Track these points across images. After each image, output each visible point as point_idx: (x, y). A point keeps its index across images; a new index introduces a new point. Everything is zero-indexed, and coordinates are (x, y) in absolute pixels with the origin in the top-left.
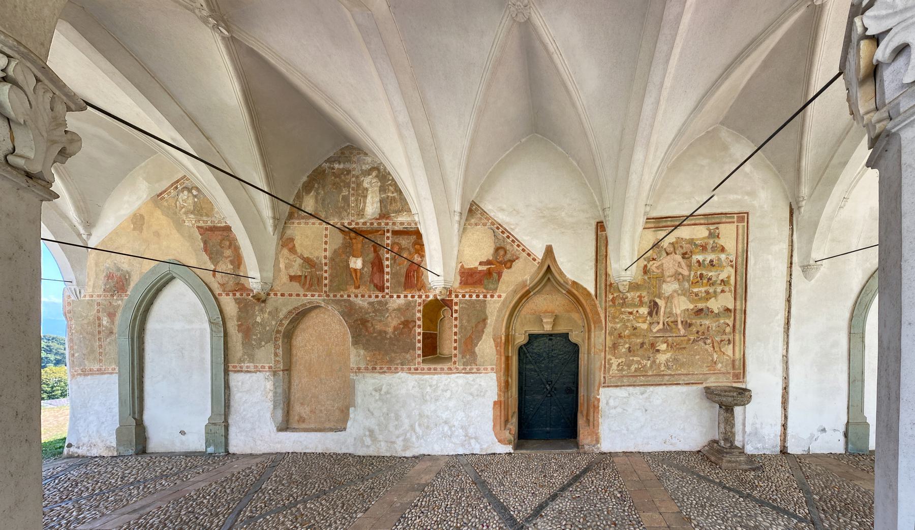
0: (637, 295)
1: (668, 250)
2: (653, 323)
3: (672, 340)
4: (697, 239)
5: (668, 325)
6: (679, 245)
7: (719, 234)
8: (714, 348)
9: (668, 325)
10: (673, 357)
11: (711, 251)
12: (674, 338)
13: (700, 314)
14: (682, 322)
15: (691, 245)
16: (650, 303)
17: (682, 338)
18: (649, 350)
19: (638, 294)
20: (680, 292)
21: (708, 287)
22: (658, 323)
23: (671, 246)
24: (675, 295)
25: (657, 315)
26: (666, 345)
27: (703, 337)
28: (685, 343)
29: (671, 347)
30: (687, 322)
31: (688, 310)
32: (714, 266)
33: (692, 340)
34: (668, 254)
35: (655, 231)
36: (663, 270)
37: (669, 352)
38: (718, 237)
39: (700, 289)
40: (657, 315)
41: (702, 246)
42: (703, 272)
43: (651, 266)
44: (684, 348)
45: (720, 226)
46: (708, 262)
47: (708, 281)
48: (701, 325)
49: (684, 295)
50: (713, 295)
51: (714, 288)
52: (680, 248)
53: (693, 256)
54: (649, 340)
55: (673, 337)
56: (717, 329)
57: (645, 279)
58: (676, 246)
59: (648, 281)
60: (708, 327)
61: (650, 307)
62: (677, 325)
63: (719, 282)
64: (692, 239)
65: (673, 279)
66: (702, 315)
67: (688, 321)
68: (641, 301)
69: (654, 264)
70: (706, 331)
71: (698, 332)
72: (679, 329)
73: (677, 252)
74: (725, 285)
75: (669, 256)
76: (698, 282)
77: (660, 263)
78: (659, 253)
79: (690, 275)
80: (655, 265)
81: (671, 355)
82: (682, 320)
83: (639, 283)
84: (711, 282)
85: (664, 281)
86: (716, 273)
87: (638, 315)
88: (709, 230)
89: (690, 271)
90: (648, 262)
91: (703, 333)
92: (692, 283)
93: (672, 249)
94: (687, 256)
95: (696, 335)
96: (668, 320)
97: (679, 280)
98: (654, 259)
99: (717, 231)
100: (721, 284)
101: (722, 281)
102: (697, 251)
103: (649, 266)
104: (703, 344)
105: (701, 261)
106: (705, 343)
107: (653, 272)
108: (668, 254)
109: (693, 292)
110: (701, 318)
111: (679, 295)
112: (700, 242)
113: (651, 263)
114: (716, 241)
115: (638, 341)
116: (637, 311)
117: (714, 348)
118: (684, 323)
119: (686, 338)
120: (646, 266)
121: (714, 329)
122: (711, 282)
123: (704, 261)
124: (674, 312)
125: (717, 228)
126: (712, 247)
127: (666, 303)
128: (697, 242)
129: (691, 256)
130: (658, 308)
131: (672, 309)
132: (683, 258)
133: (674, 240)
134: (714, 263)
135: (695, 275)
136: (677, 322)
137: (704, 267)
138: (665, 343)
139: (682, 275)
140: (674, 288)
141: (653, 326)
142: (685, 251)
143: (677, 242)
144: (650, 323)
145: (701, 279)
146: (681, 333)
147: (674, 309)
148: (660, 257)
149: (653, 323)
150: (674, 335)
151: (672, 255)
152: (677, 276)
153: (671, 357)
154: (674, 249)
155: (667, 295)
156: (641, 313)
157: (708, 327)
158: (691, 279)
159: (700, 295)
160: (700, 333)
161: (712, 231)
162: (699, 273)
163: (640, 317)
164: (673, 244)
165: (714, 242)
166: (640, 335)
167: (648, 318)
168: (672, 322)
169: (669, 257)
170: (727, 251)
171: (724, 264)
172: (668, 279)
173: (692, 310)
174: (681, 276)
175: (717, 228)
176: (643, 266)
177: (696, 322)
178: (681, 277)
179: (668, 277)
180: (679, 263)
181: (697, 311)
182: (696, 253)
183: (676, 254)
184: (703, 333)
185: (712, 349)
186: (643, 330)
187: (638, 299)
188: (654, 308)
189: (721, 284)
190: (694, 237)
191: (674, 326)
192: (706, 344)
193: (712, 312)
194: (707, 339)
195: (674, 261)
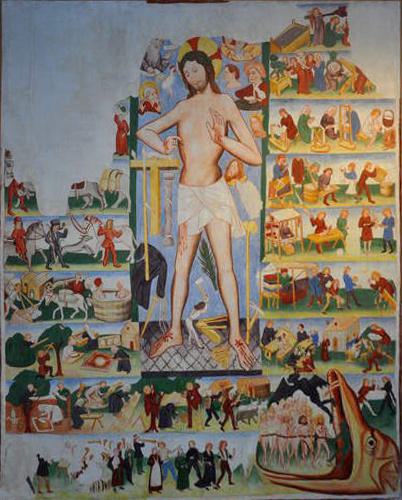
7: (347, 30)
32: (335, 136)
68: (108, 245)
76: (288, 188)
84: (328, 189)
94: (251, 99)
99: (342, 20)
123: (305, 119)
132: (243, 105)
134: (336, 128)
136: (227, 323)
145: (298, 180)
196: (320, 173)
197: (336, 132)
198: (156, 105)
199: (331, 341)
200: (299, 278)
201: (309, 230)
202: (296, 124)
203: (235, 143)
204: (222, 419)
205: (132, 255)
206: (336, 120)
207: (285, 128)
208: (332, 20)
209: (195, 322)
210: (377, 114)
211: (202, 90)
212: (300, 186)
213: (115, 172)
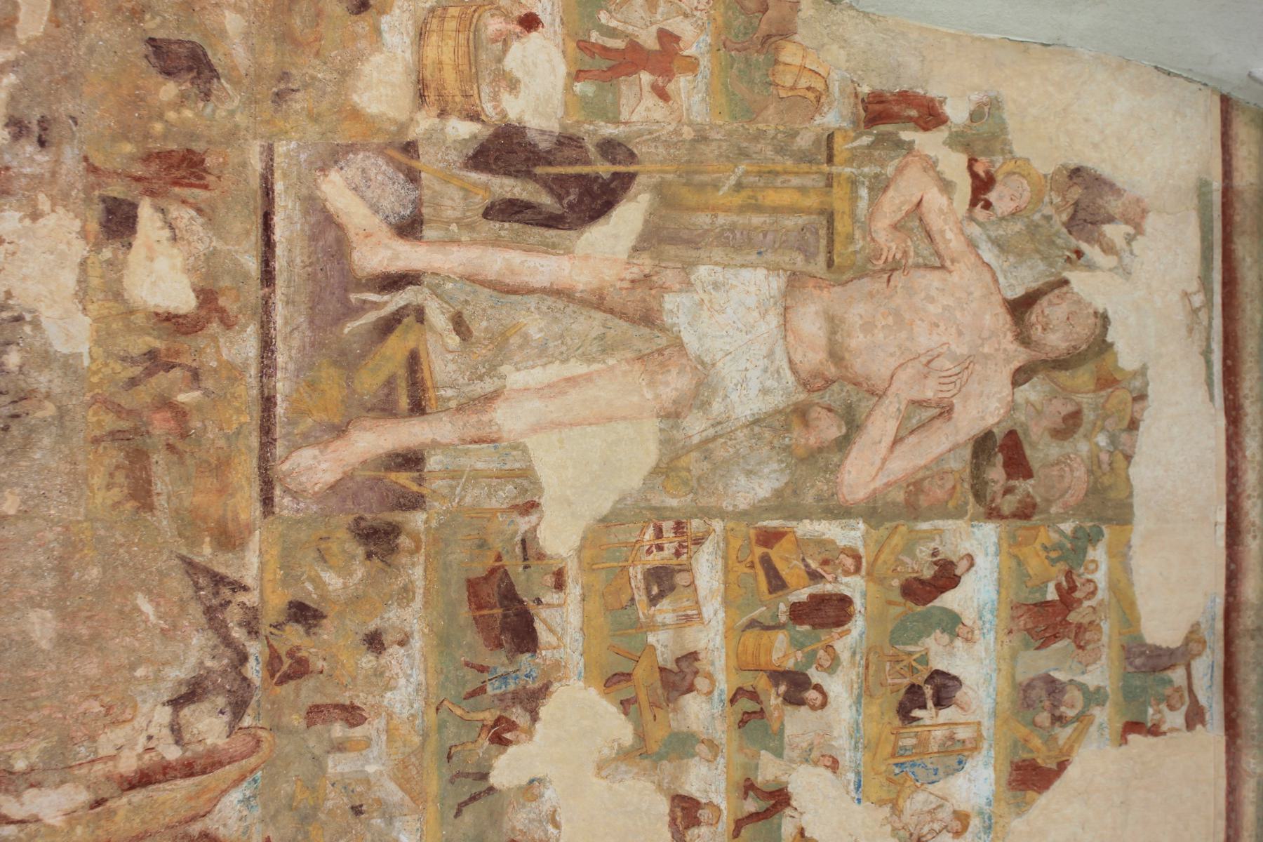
0: (682, 27)
1: (1052, 311)
2: (413, 177)
3: (234, 372)
4: (1121, 554)
5: (388, 326)
6: (1086, 400)
7: (1155, 731)
8: (143, 779)
9: (388, 326)
10: (42, 380)
11: (1022, 678)
12: (249, 389)
13: (481, 624)
14: (411, 460)
15: (1081, 509)
16: (609, 148)
17: (245, 469)
18: (124, 135)
19: (695, 42)
20: (695, 426)
21: (724, 685)
22: (409, 228)
23: (1083, 330)
24: (675, 384)
25: (488, 213)
26: (182, 300)
27: (254, 670)
28: (200, 497)
29: (155, 362)
30: (415, 502)
31: (530, 507)
32: (904, 712)
33: (223, 565)
34: (1020, 308)
35: (1202, 188)
36: (893, 268)
37: (102, 337)
38: (1134, 727)
39: (713, 609)
40: (488, 213)
41: (1068, 598)
42: (857, 626)
43: (930, 165)
44: (142, 494)
45: (1212, 735)
46: (939, 663)
47: (777, 676)
48: (375, 642)
49: (665, 471)
50: (658, 733)
51: (721, 731)
52: (1062, 408)
53: (989, 532)
54: (232, 135)
55: (267, 368)
56: (335, 800)
57: (818, 100)
58: (1083, 377)
59: (804, 141)
60: (352, 715)
61: (568, 141)
62: (385, 409)
63: (769, 770)
64: (1122, 514)
65: (813, 358)
66: (472, 644)
67: (417, 520)
69: (946, 186)
70: (308, 692)
71: (303, 613)
72: (339, 431)
73: (1031, 392)
74: (739, 825)
75: (1005, 319)
76: (777, 583)
77: (952, 240)
78: (1033, 229)
79: (839, 512)
80: (935, 199)
81: (68, 365)
82: (433, 462)
83: (790, 54)
84: (773, 700)
85: (795, 281)
86: (842, 743)
87: (494, 25)
88: (1183, 655)
89: (873, 512)
90: (961, 141)
91: (300, 669)
92: (769, 538)
93: (1056, 341)
94: (996, 473)
95: (277, 601)
96: (438, 317)
97: (801, 413)
98: (982, 185)
99: (1176, 719)
100: (749, 787)
101: (779, 799)
102: (1035, 564)
103: (928, 142)
104: (178, 674)
105: (949, 600)
106: (190, 694)
107: (880, 186)
108: (1020, 308)
109: (689, 542)
110: (444, 641)
111: (672, 416)
112: (1100, 577)
113: (954, 165)
114: (1101, 715)
115: (233, 22)
116: (530, 22)
117: (143, 779)
118: (404, 479)
119: (246, 504)
120: (931, 116)
121: (338, 765)
122: (773, 700)
123: (952, 623)
124: (515, 378)
125: (1195, 717)
126: (1053, 688)
127: (597, 302)
128: (1098, 553)
129: (993, 514)
130: (552, 221)
131: (543, 353)
132: (983, 445)
133: (1126, 357)
134: (926, 715)
135: (830, 556)
136: (418, 408)
137: (903, 632)
138: (207, 296)
139: (844, 443)
140: (728, 371)
141: (379, 169)
142: (1034, 456)
143: (1107, 381)
144: (410, 148)
145: (798, 613)
146: (306, 456)
147: (538, 375)
148: (1001, 245)
149: (413, 177)
150: (282, 386)
151: (1008, 342)
152: (835, 396)
153: (46, 358)
154: (1060, 364)
155: (675, 308)
156: (512, 62)
157: (352, 715)
158: (806, 528)
159: (665, 611)
160: (294, 635)
161: (1178, 675)
162: (852, 586)
163: (474, 45)
164: (1100, 346)
165: (1094, 697)
166: (286, 38)
167: (462, 129)
168: (414, 361)
169: (998, 319)
170: (1021, 807)
171: (917, 803)
172: (809, 322)
173: (528, 548)
174: (830, 429)
175: (1195, 717)
176: (934, 92)
177: (406, 594)
178: (830, 429)
179: (834, 324)
180: (946, 411)
181: (509, 596)
182: (1012, 548)
183: (1020, 376)
184: (300, 669)
185: (128, 764)
186: (346, 73)
187: (648, 40)
188: (557, 185)
189: (749, 787)
190: (1143, 522)
191: (369, 382)
192: (177, 703)
193: (500, 735)
194: (238, 707)
195: (967, 363)
196: (816, 676)
197: (917, 713)
198: (988, 205)
199: (358, 732)
200: (538, 625)
201: (664, 645)
202: (938, 602)
203: (891, 427)
204: (125, 400)
205: (609, 130)
206: (947, 714)
207: (928, 574)
208: (1178, 689)
209: (420, 315)
210: (956, 825)
211: (1024, 339)
212: (783, 619)
213: (819, 86)
